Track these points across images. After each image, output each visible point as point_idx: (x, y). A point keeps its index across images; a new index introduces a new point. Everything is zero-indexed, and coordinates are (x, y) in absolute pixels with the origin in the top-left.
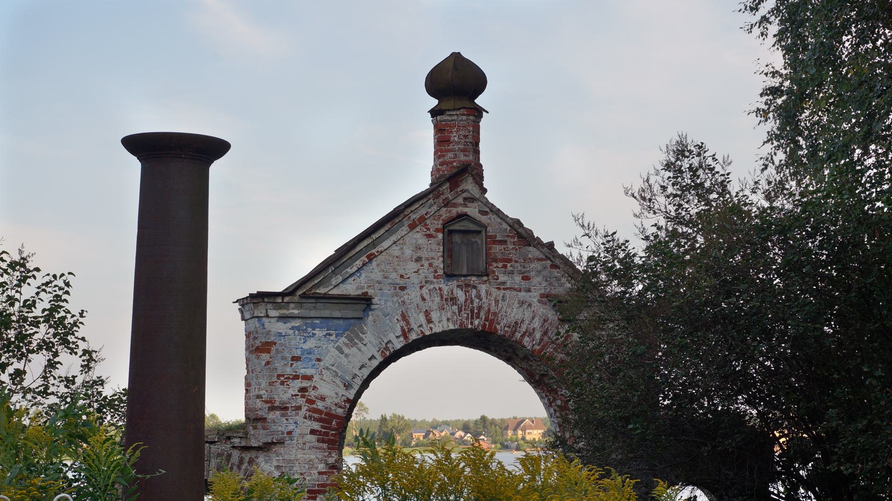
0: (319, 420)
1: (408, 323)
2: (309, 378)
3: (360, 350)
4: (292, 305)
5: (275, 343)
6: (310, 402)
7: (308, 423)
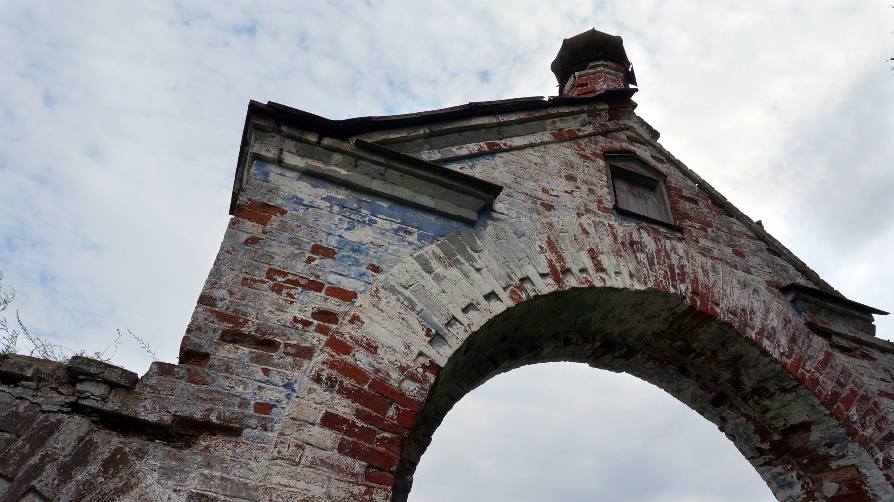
0: (353, 395)
1: (560, 258)
2: (348, 296)
3: (466, 275)
4: (337, 157)
5: (283, 212)
6: (338, 345)
7: (322, 394)
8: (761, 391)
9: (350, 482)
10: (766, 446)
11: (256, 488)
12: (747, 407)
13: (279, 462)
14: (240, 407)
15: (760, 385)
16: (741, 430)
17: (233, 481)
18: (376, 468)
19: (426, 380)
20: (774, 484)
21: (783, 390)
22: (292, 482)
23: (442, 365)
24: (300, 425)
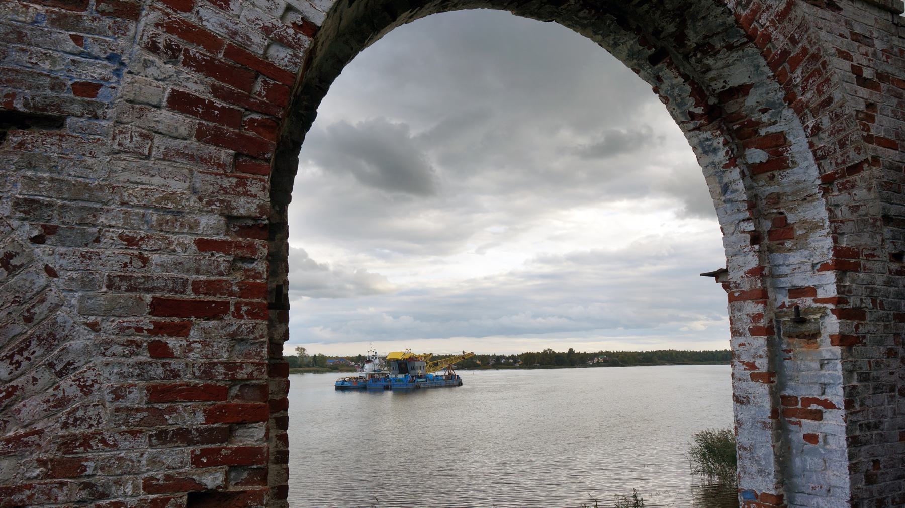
0: (207, 68)
7: (163, 67)
8: (706, 48)
9: (216, 174)
10: (699, 110)
11: (101, 188)
12: (688, 66)
13: (123, 156)
14: (52, 89)
15: (706, 41)
16: (676, 91)
17: (68, 183)
18: (247, 156)
19: (299, 44)
20: (700, 150)
21: (730, 48)
22: (145, 179)
23: (319, 22)
24: (141, 109)
